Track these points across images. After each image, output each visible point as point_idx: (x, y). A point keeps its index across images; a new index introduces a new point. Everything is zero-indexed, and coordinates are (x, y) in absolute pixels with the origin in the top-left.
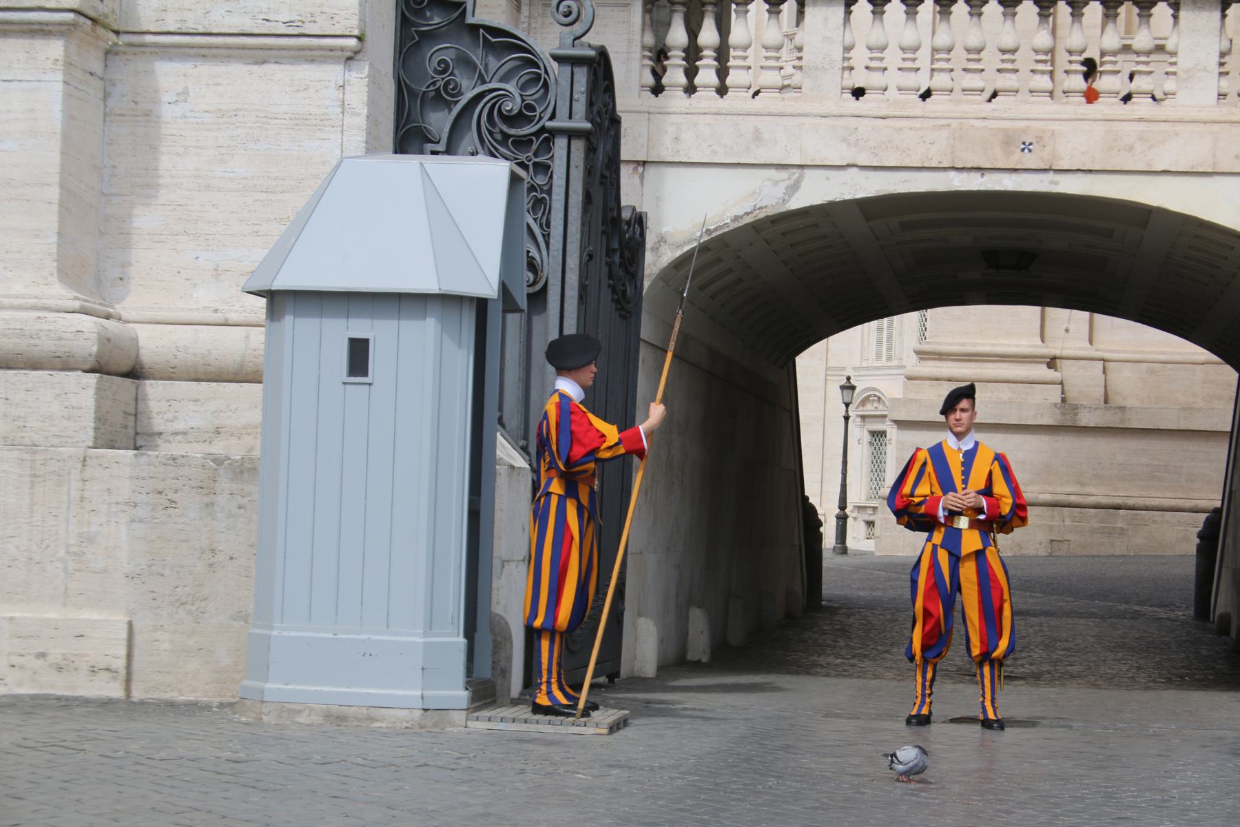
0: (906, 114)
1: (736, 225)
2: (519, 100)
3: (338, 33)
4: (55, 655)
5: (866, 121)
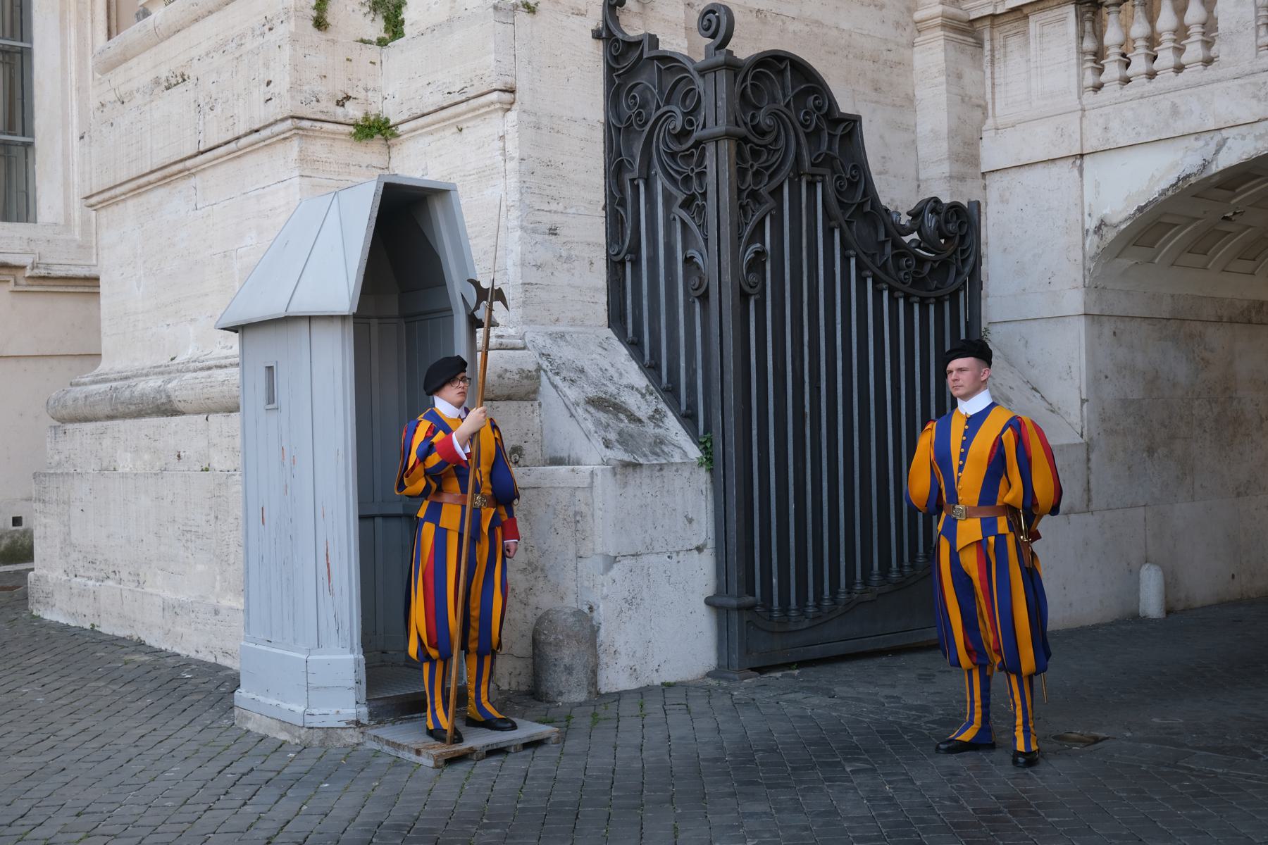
1: (1163, 198)
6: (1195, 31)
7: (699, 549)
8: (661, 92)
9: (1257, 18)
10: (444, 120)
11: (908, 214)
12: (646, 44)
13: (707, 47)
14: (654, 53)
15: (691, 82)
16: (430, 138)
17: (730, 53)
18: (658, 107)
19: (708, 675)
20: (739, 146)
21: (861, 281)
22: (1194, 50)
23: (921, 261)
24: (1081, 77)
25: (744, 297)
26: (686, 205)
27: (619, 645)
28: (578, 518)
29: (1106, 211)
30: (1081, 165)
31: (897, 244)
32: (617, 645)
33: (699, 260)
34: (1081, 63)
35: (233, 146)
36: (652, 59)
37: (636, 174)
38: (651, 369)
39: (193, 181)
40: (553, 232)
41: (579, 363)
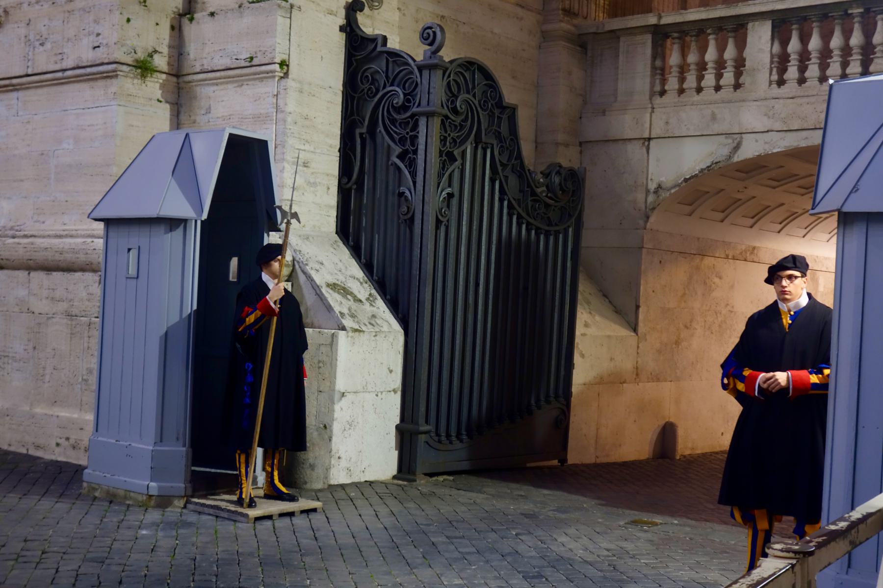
0: (806, 94)
2: (402, 96)
3: (267, 62)
4: (73, 437)
5: (781, 101)
6: (730, 64)
7: (395, 391)
8: (387, 77)
9: (772, 62)
10: (229, 77)
11: (541, 173)
12: (380, 42)
13: (425, 52)
14: (384, 49)
15: (411, 73)
16: (215, 88)
17: (441, 57)
18: (384, 87)
19: (394, 477)
20: (442, 120)
21: (510, 216)
22: (728, 77)
23: (547, 206)
24: (652, 85)
25: (438, 222)
26: (401, 157)
27: (342, 453)
28: (321, 365)
29: (663, 179)
30: (649, 145)
31: (534, 194)
32: (340, 452)
33: (407, 193)
34: (653, 75)
35: (60, 75)
36: (382, 52)
37: (364, 130)
38: (367, 267)
39: (14, 95)
40: (305, 165)
41: (320, 259)
